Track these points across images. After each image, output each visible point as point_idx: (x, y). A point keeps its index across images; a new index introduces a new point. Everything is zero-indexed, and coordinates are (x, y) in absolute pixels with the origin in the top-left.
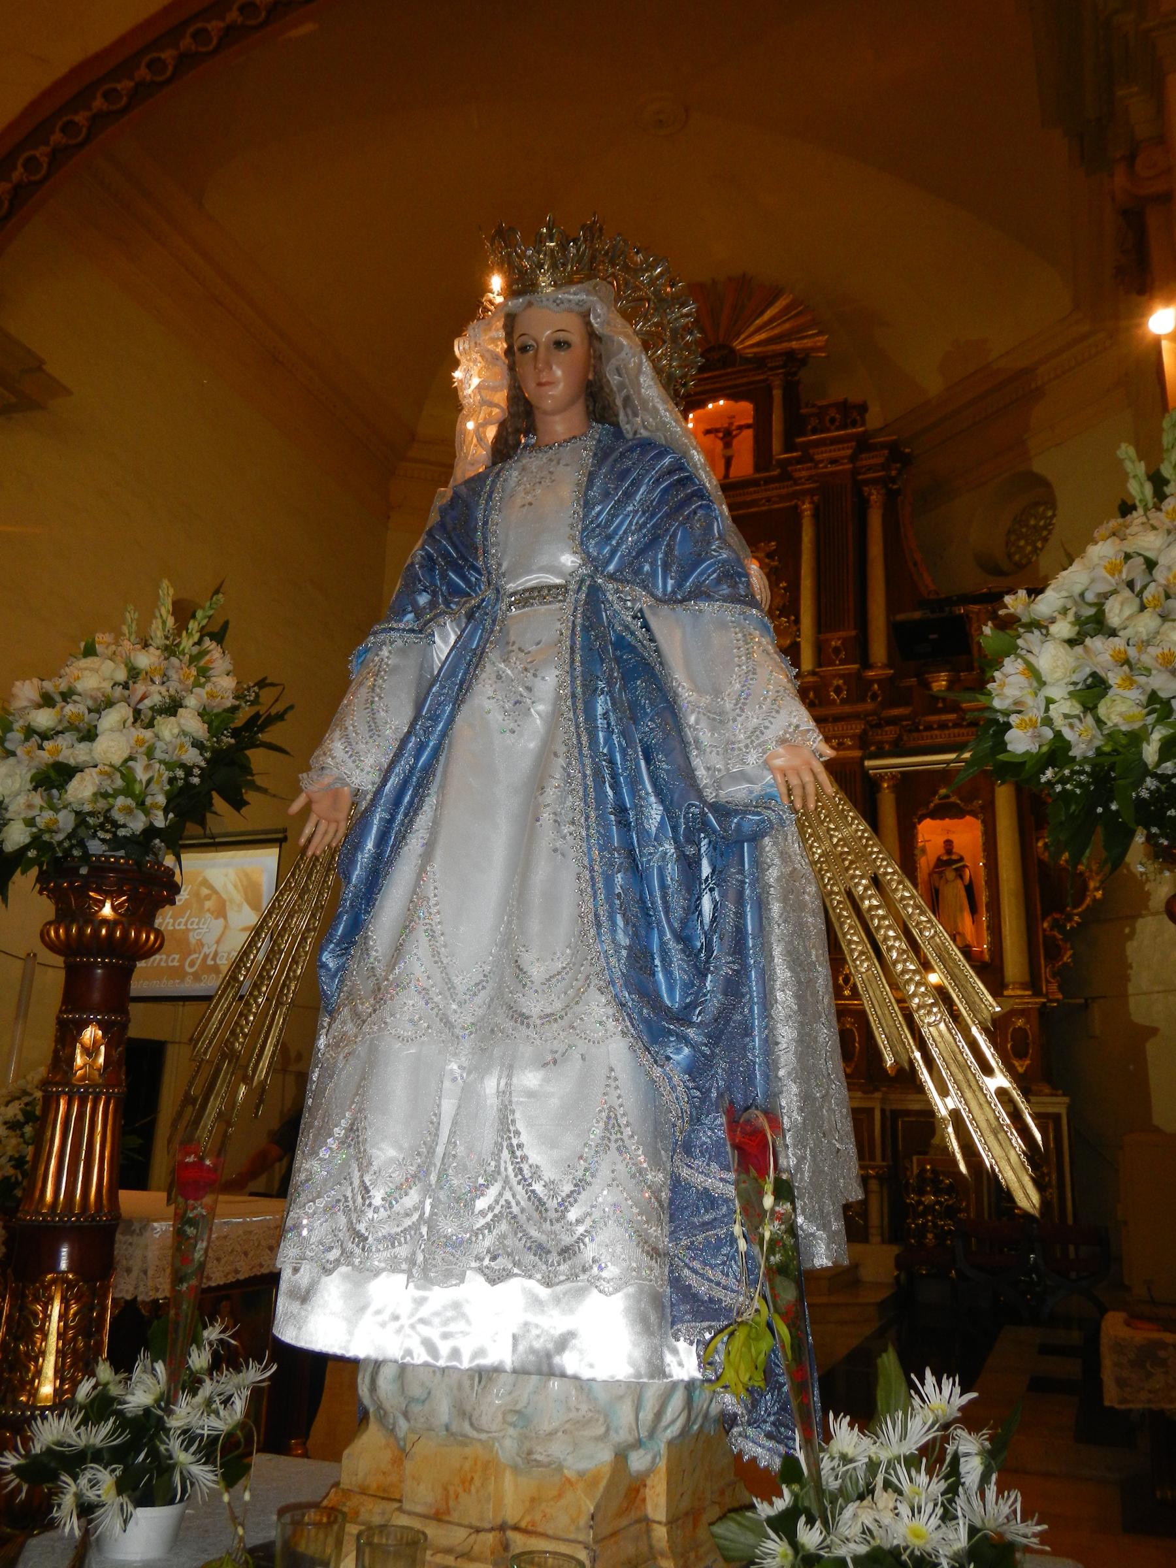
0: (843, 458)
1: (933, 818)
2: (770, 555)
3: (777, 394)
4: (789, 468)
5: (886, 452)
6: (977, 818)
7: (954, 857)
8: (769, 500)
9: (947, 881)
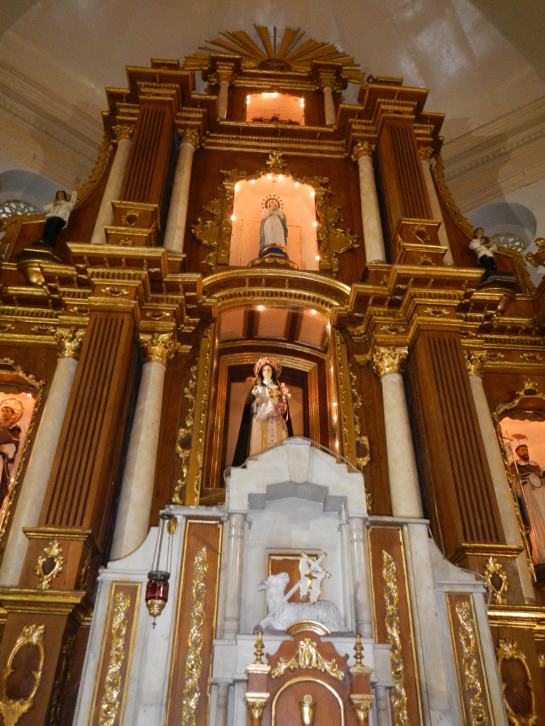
0: (404, 112)
1: (512, 417)
2: (324, 185)
3: (327, 91)
4: (350, 120)
5: (433, 126)
7: (532, 464)
8: (321, 152)
9: (533, 487)
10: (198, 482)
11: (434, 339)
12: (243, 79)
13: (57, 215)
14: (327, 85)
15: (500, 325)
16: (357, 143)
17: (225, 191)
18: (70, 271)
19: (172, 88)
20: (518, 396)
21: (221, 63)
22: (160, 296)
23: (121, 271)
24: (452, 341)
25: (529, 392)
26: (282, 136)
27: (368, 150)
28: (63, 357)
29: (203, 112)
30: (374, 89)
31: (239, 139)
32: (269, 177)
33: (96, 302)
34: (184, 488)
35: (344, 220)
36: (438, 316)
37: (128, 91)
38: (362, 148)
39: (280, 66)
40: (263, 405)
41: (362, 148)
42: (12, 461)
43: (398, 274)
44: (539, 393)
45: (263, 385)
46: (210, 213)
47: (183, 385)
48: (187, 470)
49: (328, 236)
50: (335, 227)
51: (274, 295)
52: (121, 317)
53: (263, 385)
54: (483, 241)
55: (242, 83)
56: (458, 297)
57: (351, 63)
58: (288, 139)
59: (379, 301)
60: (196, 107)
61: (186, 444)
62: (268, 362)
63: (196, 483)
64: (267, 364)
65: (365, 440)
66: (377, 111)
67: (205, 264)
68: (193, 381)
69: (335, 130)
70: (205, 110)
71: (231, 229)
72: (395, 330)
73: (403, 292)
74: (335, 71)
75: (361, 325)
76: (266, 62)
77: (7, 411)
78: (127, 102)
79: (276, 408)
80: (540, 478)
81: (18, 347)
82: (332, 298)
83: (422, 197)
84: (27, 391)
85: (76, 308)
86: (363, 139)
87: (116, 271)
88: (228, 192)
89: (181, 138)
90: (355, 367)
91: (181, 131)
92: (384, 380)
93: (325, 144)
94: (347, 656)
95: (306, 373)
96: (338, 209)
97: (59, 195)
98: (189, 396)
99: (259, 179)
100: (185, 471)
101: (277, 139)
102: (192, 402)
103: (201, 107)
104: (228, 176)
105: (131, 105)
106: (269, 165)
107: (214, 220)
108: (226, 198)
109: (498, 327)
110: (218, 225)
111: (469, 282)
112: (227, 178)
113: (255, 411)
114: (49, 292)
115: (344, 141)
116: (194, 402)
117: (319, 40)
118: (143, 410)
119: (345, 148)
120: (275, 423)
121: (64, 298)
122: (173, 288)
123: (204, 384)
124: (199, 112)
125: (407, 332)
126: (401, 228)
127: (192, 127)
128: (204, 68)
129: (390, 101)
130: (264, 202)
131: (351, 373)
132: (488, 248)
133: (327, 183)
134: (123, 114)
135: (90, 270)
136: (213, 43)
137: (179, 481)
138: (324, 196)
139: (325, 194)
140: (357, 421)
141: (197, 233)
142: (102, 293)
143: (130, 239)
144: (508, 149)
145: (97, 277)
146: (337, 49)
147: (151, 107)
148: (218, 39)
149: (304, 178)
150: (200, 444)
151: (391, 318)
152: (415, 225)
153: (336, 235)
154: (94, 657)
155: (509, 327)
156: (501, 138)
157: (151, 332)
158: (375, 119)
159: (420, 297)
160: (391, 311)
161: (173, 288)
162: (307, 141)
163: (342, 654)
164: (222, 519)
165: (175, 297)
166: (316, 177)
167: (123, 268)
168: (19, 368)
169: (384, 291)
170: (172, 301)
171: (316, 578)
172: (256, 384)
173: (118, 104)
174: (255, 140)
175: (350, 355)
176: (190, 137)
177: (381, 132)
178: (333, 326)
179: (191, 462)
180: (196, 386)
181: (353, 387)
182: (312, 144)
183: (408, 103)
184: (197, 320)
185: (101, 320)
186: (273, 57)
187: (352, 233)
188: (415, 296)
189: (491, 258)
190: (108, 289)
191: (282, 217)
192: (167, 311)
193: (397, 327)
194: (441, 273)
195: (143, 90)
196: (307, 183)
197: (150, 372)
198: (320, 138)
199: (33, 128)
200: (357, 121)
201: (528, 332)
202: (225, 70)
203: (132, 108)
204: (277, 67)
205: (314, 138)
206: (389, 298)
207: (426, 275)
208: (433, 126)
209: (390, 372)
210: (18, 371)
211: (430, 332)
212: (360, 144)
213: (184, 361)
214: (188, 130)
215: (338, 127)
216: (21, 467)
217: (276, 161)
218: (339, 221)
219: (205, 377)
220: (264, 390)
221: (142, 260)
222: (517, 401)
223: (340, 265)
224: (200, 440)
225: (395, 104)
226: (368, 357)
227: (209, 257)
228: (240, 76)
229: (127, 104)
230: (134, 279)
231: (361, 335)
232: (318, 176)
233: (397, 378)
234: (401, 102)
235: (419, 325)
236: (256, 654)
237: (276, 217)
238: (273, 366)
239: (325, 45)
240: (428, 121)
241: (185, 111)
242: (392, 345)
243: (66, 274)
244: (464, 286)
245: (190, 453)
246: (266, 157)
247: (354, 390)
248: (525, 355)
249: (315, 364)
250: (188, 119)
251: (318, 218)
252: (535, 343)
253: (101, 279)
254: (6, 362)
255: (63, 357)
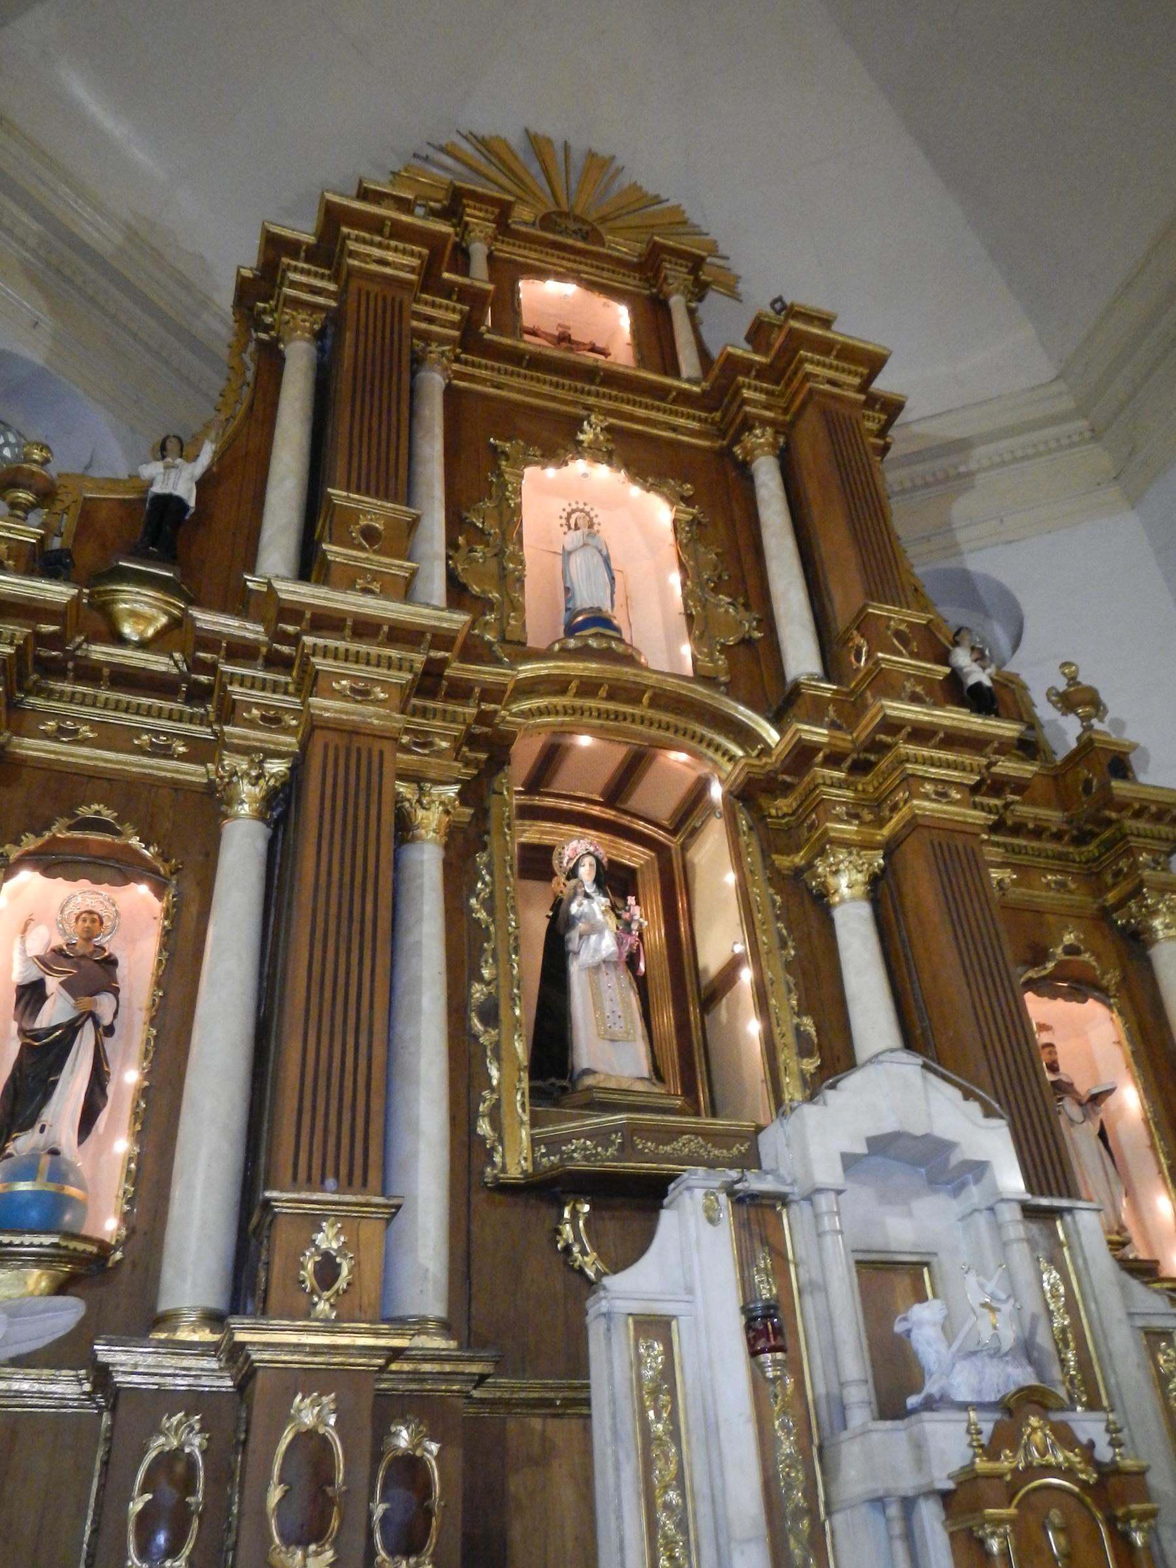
0: (845, 384)
2: (688, 501)
3: (677, 303)
4: (741, 379)
5: (884, 417)
6: (1110, 1007)
7: (1064, 1079)
8: (674, 429)
10: (523, 1095)
11: (940, 844)
12: (508, 244)
13: (177, 493)
14: (677, 291)
15: (1017, 820)
16: (750, 429)
17: (504, 486)
18: (252, 631)
19: (412, 254)
20: (1054, 954)
21: (471, 203)
22: (430, 704)
23: (374, 650)
24: (969, 849)
25: (1071, 950)
26: (603, 383)
27: (774, 445)
28: (237, 817)
29: (461, 312)
30: (797, 330)
31: (519, 375)
32: (580, 466)
33: (326, 709)
34: (496, 1106)
35: (730, 577)
36: (944, 800)
37: (311, 240)
38: (762, 440)
39: (580, 230)
40: (593, 938)
41: (762, 440)
42: (110, 1030)
43: (885, 716)
44: (1086, 951)
45: (587, 896)
46: (477, 527)
47: (465, 893)
48: (499, 1070)
49: (704, 607)
50: (716, 590)
51: (621, 718)
52: (377, 745)
53: (587, 896)
54: (976, 655)
55: (508, 250)
56: (976, 770)
57: (713, 249)
58: (614, 393)
59: (833, 760)
60: (449, 297)
61: (490, 1015)
62: (592, 849)
63: (519, 1097)
64: (589, 853)
65: (808, 1024)
66: (795, 373)
67: (478, 636)
68: (484, 883)
69: (704, 393)
70: (467, 308)
71: (524, 569)
72: (857, 816)
73: (887, 747)
74: (690, 265)
75: (785, 797)
76: (554, 217)
77: (93, 921)
78: (307, 261)
79: (620, 943)
80: (1080, 1104)
81: (109, 780)
82: (728, 738)
83: (893, 563)
84: (138, 879)
85: (255, 711)
86: (765, 422)
87: (364, 648)
88: (510, 488)
89: (417, 361)
90: (776, 878)
91: (419, 344)
92: (838, 914)
93: (682, 416)
94: (1091, 1445)
95: (632, 872)
96: (716, 554)
97: (169, 445)
98: (482, 915)
99: (564, 469)
100: (494, 1072)
101: (593, 388)
102: (487, 928)
103: (459, 300)
104: (503, 453)
105: (313, 268)
106: (582, 442)
107: (487, 545)
108: (507, 500)
109: (1015, 823)
110: (496, 555)
111: (1001, 744)
112: (503, 457)
113: (573, 946)
114: (185, 668)
115: (717, 415)
116: (492, 929)
117: (650, 189)
118: (419, 943)
119: (719, 429)
120: (612, 974)
121: (229, 688)
122: (460, 691)
123: (508, 893)
124: (454, 310)
125: (880, 823)
126: (862, 622)
127: (443, 340)
128: (432, 204)
129: (821, 358)
130: (565, 515)
131: (771, 891)
132: (984, 668)
133: (691, 496)
134: (294, 285)
135: (308, 640)
136: (442, 150)
137: (486, 1093)
138: (690, 523)
139: (692, 520)
140: (792, 987)
141: (460, 568)
142: (334, 690)
143: (374, 580)
144: (973, 466)
145: (324, 657)
146: (686, 215)
147: (374, 288)
148: (453, 143)
149: (650, 480)
150: (518, 1020)
151: (850, 794)
152: (890, 618)
153: (718, 606)
154: (628, 1457)
155: (1031, 826)
156: (962, 446)
157: (415, 778)
158: (787, 385)
159: (916, 762)
160: (852, 779)
161: (460, 691)
162: (649, 401)
163: (1084, 1439)
164: (791, 1197)
165: (459, 709)
166: (671, 481)
167: (378, 645)
168: (128, 828)
169: (845, 740)
170: (454, 718)
171: (999, 1310)
172: (575, 895)
173: (285, 260)
174: (551, 384)
175: (765, 855)
176: (439, 363)
177: (799, 414)
178: (729, 795)
179: (504, 1054)
180: (491, 893)
181: (778, 918)
182: (658, 409)
183: (853, 368)
184: (483, 756)
185: (337, 748)
186: (565, 207)
187: (746, 606)
188: (908, 761)
189: (989, 689)
190: (344, 682)
191: (604, 552)
192: (444, 737)
193: (859, 810)
194: (955, 723)
195: (352, 245)
196: (656, 491)
197: (422, 862)
198: (674, 402)
199: (28, 255)
200: (754, 382)
201: (1058, 837)
202: (479, 221)
203: (316, 275)
204: (575, 232)
205: (663, 399)
206: (855, 756)
207: (931, 723)
208: (884, 417)
209: (853, 899)
210: (130, 838)
211: (935, 832)
212: (758, 432)
213: (460, 838)
214: (433, 347)
215: (712, 387)
216: (150, 1048)
217: (595, 435)
218: (720, 577)
219: (507, 877)
220: (589, 904)
221: (422, 634)
222: (1050, 965)
223: (731, 670)
224: (517, 1012)
225: (831, 367)
226: (798, 859)
227: (487, 623)
228: (504, 235)
229: (306, 266)
230: (400, 669)
231: (785, 815)
232: (673, 479)
233: (864, 910)
234: (841, 364)
235: (915, 816)
236: (970, 1445)
237: (594, 551)
238: (601, 856)
239: (660, 202)
240: (878, 407)
241: (426, 303)
242: (855, 846)
243: (244, 638)
244: (989, 750)
245: (499, 1034)
246: (576, 424)
247: (780, 925)
248: (1049, 877)
249: (653, 854)
250: (430, 320)
251: (682, 567)
252: (1060, 856)
253: (331, 662)
254: (98, 812)
255: (237, 817)
